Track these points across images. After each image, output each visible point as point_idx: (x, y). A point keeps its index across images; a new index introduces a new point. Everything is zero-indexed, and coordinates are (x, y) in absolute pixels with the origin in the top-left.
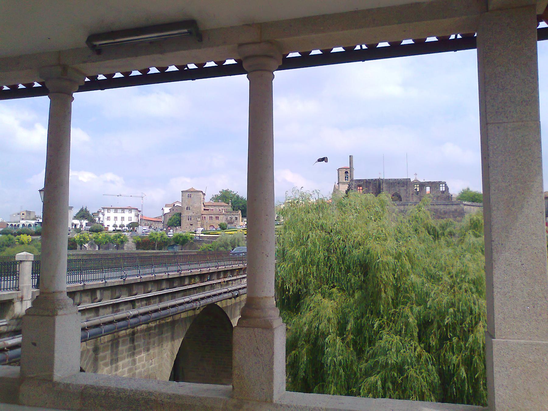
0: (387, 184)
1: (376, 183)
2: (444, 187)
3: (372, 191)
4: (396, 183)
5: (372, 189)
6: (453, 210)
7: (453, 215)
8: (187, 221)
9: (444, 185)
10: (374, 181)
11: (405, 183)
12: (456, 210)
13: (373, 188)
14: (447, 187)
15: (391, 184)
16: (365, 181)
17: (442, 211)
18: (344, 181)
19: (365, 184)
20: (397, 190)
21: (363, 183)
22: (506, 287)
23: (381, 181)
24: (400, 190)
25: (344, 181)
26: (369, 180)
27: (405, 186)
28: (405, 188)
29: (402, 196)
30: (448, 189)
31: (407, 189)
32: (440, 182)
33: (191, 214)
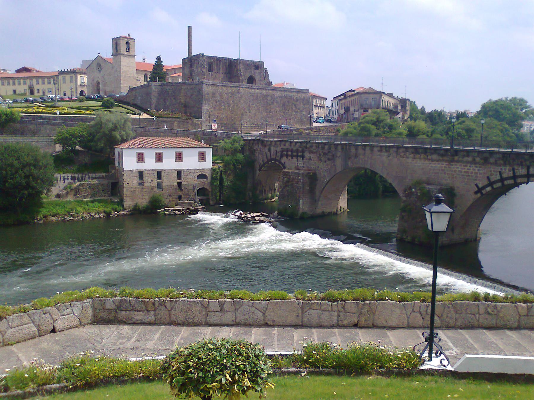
0: (243, 64)
1: (226, 63)
4: (252, 64)
6: (302, 97)
7: (303, 103)
10: (225, 60)
11: (260, 66)
12: (304, 98)
15: (248, 65)
16: (216, 59)
17: (295, 98)
18: (126, 53)
19: (216, 62)
20: (253, 73)
22: (320, 169)
23: (238, 61)
24: (255, 73)
25: (126, 53)
27: (260, 69)
29: (257, 78)
31: (261, 73)
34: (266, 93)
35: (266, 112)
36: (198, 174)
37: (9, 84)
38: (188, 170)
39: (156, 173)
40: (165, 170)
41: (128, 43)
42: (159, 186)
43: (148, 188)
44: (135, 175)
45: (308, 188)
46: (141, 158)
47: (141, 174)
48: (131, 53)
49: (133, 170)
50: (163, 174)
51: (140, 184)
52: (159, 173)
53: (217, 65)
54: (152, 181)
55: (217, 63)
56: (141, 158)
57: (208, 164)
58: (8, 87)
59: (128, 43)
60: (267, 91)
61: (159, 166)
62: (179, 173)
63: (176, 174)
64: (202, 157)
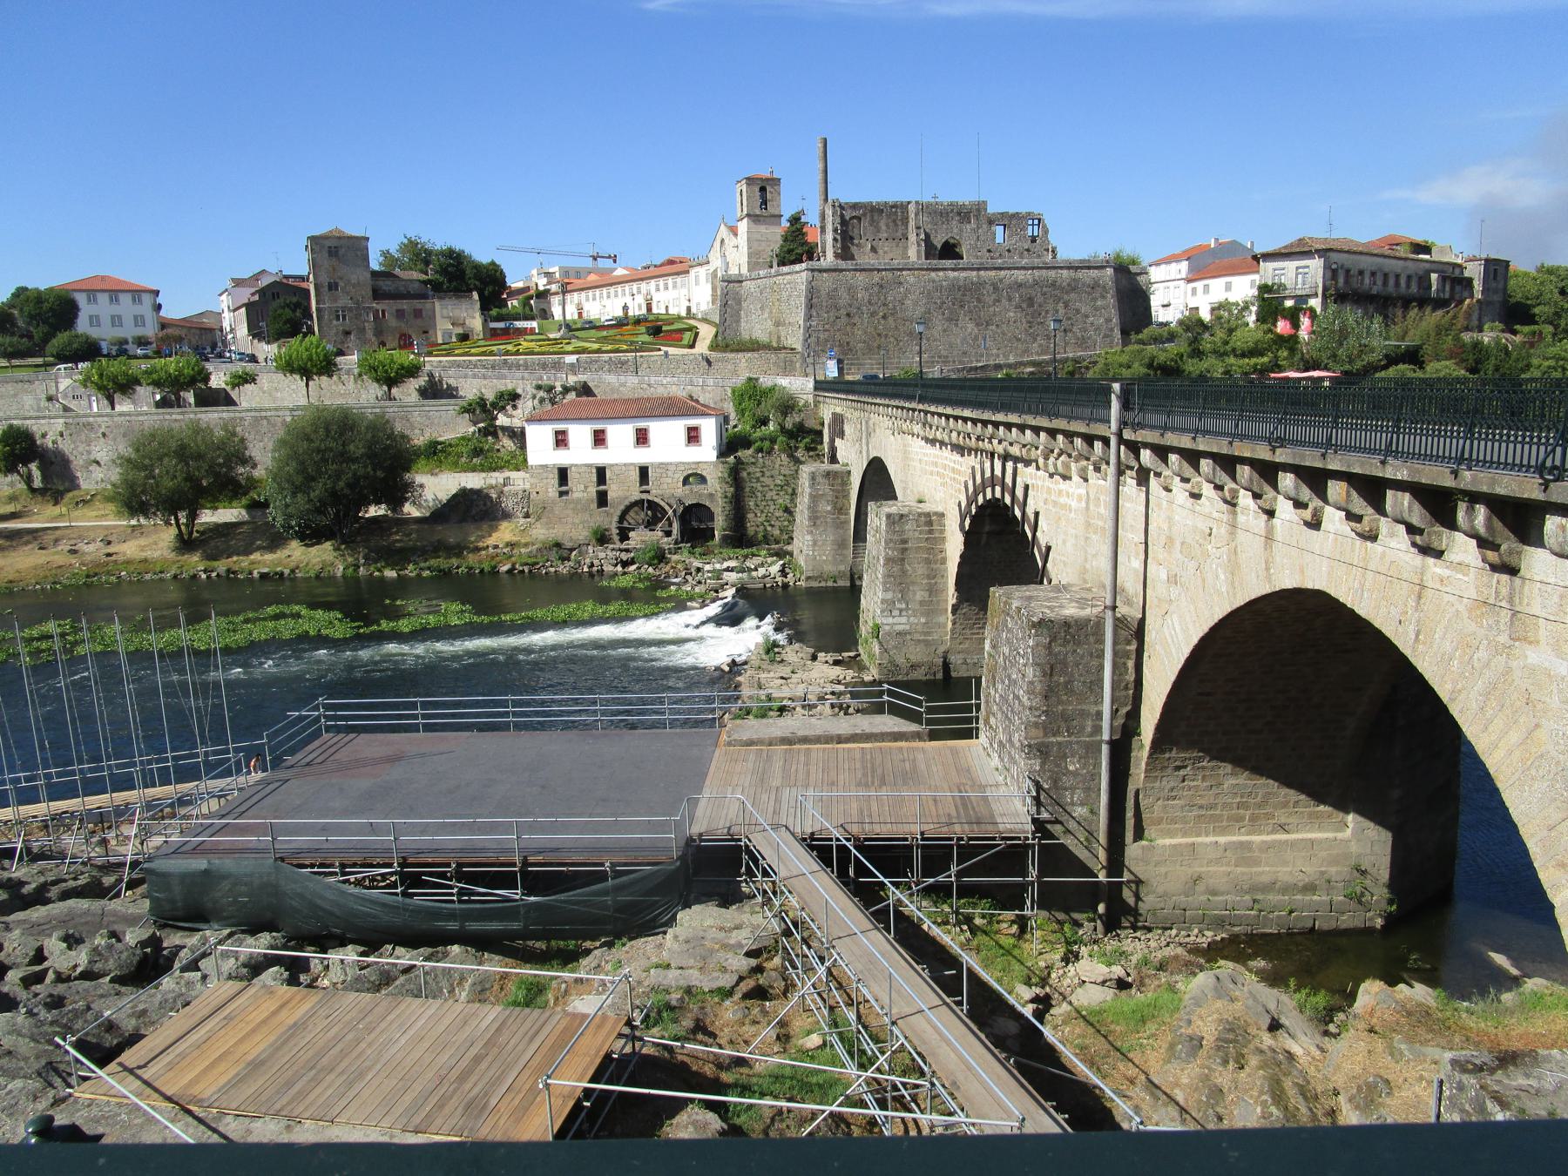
2: (1036, 227)
3: (885, 235)
5: (884, 228)
8: (335, 322)
9: (1036, 222)
10: (892, 207)
13: (887, 226)
14: (1044, 226)
21: (864, 215)
24: (961, 230)
26: (878, 203)
28: (973, 224)
30: (1046, 232)
32: (1029, 214)
33: (344, 301)
34: (978, 277)
35: (977, 325)
36: (685, 474)
37: (616, 296)
38: (664, 466)
39: (594, 471)
40: (612, 465)
41: (763, 189)
42: (602, 499)
43: (579, 501)
44: (551, 476)
45: (829, 508)
46: (561, 440)
47: (563, 474)
48: (771, 210)
49: (546, 466)
50: (608, 474)
51: (562, 494)
52: (601, 473)
53: (872, 220)
54: (586, 487)
55: (872, 216)
56: (561, 440)
57: (707, 451)
58: (615, 300)
59: (763, 189)
60: (982, 273)
61: (600, 457)
62: (644, 472)
63: (635, 475)
64: (693, 436)
